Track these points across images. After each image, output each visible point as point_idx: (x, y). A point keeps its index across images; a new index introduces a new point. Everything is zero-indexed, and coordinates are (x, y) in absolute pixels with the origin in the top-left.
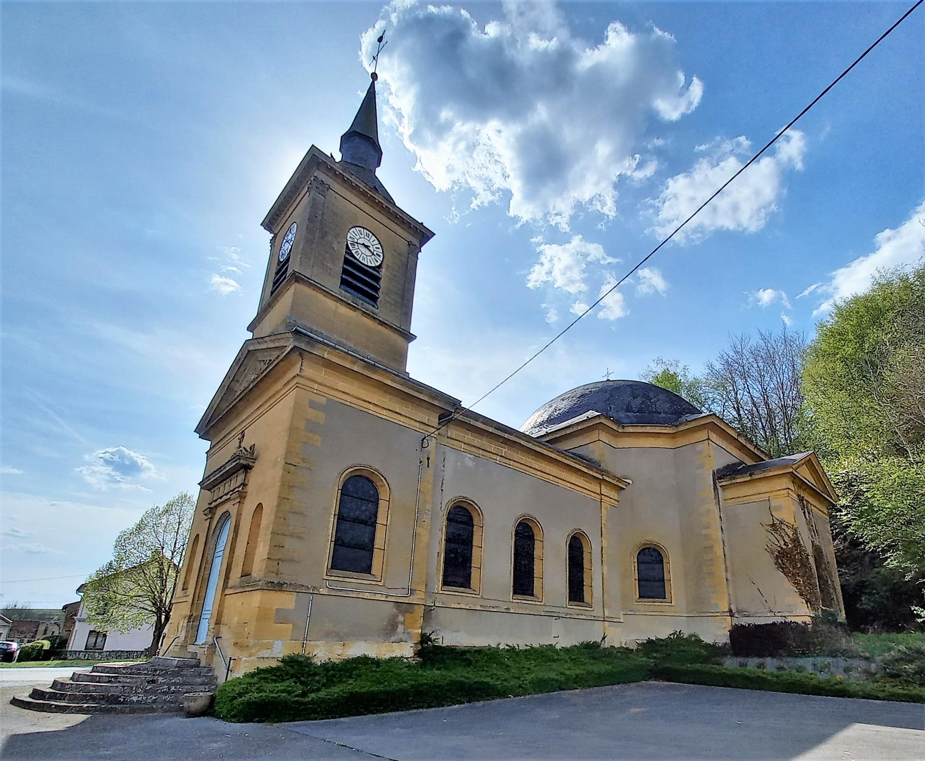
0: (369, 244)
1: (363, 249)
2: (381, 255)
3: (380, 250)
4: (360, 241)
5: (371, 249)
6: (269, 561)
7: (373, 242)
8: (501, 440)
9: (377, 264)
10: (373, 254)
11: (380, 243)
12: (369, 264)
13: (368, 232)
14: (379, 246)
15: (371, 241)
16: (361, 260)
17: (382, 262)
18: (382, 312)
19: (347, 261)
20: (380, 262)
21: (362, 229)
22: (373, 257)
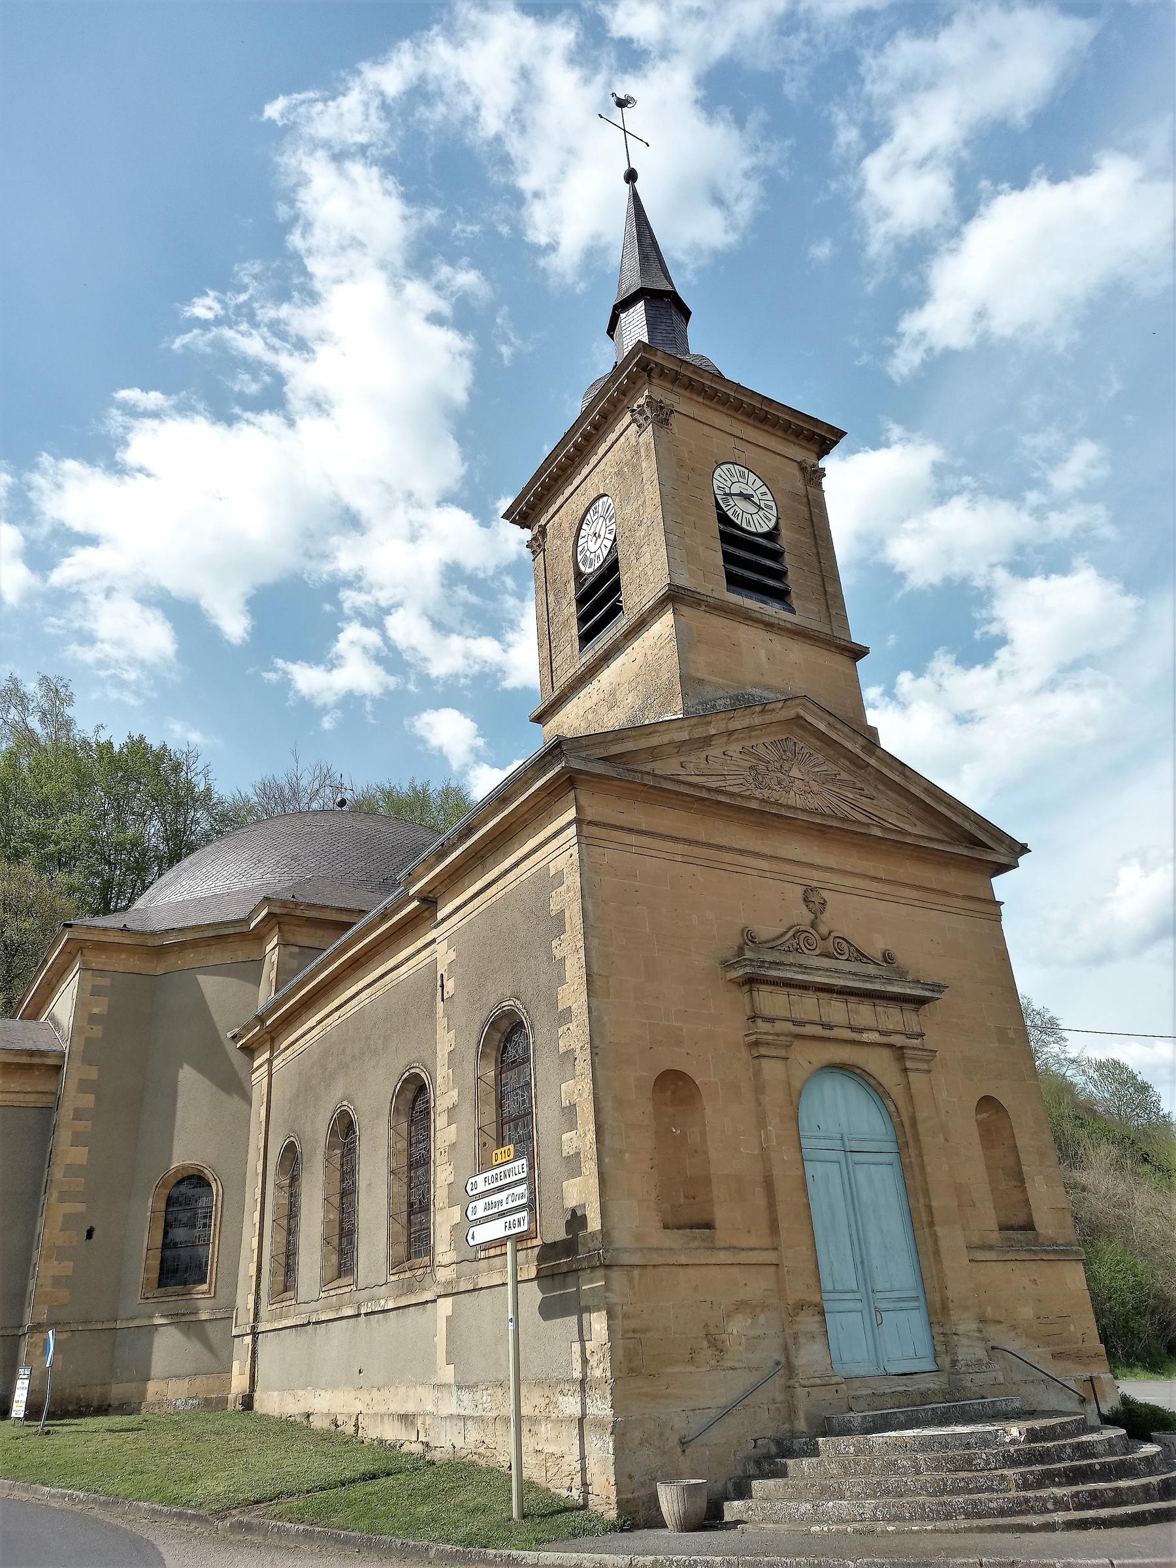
0: (750, 492)
1: (742, 504)
2: (773, 504)
3: (769, 497)
4: (735, 489)
5: (755, 499)
6: (973, 1264)
7: (753, 485)
8: (691, 369)
9: (772, 524)
10: (760, 508)
11: (765, 484)
12: (760, 530)
13: (741, 468)
14: (764, 489)
15: (750, 484)
16: (744, 526)
17: (778, 518)
18: (804, 613)
19: (725, 538)
20: (774, 520)
21: (731, 466)
22: (761, 513)
